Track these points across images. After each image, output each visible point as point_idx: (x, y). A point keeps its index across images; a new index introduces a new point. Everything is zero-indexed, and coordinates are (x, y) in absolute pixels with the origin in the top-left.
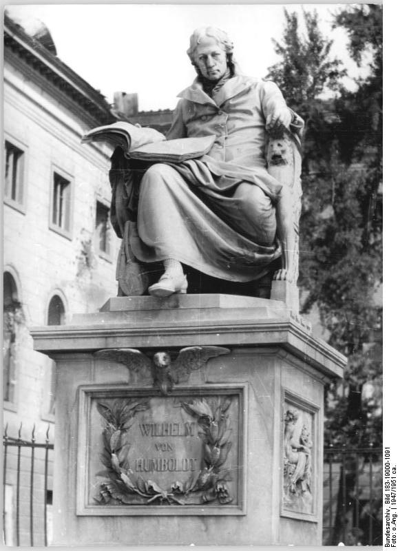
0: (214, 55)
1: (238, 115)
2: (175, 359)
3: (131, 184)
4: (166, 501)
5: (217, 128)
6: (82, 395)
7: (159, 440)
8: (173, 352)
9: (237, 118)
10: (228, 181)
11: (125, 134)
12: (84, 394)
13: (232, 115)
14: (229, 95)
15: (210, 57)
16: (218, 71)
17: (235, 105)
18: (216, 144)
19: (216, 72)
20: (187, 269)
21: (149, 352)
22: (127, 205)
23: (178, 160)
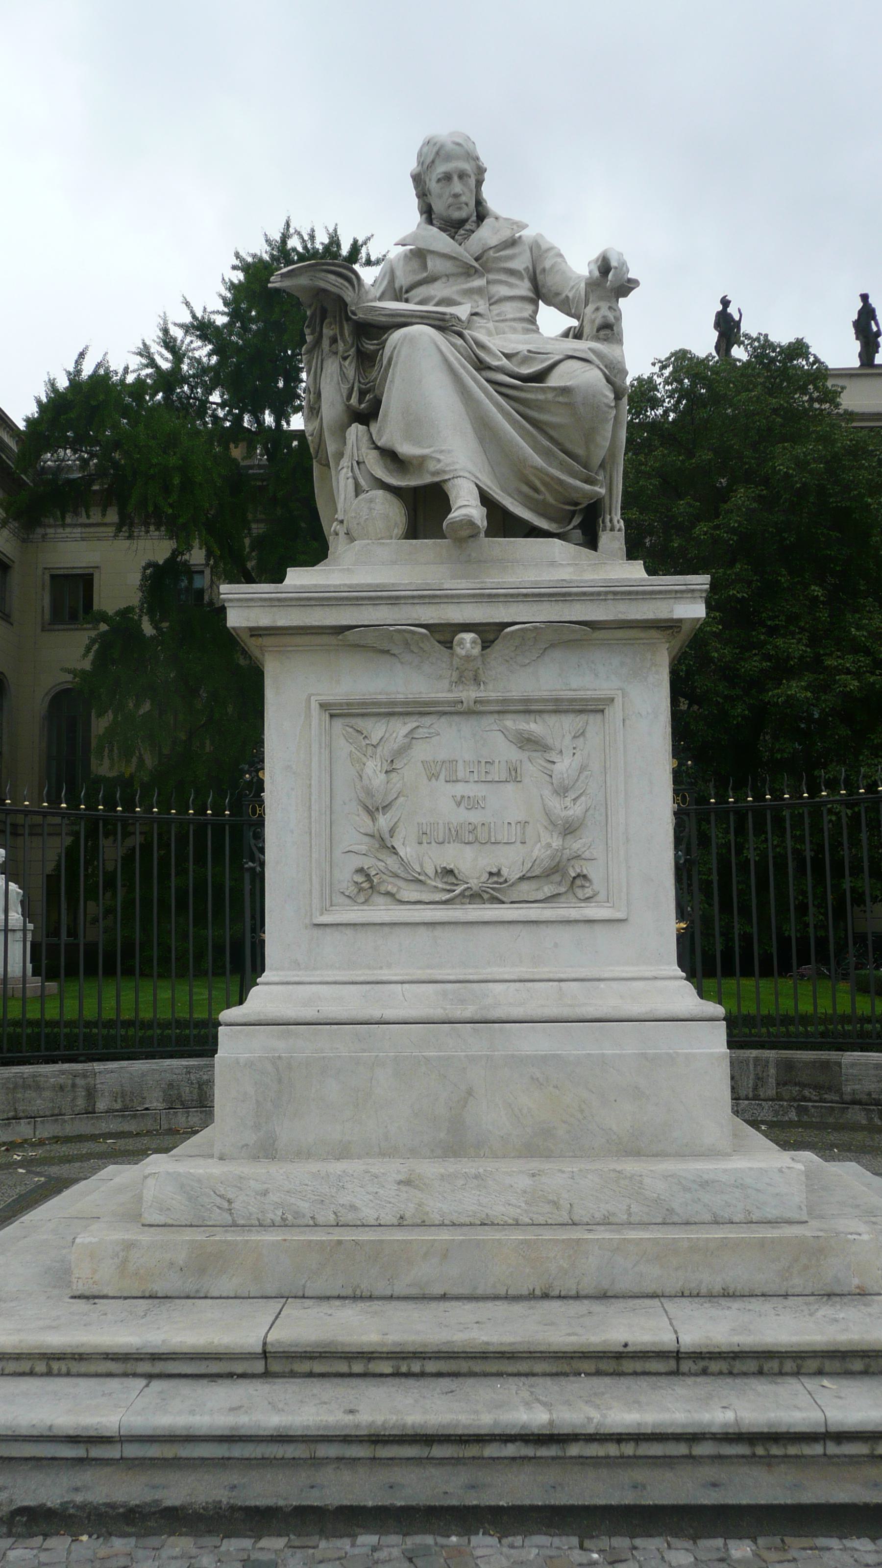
0: (462, 176)
1: (503, 277)
2: (489, 647)
3: (354, 365)
4: (475, 897)
5: (469, 292)
6: (314, 706)
7: (460, 789)
8: (490, 634)
9: (500, 282)
10: (531, 357)
11: (350, 274)
12: (318, 706)
13: (491, 277)
14: (493, 241)
15: (456, 178)
16: (467, 204)
17: (499, 259)
18: (474, 317)
19: (464, 206)
20: (486, 499)
21: (444, 634)
22: (349, 397)
23: (443, 320)
